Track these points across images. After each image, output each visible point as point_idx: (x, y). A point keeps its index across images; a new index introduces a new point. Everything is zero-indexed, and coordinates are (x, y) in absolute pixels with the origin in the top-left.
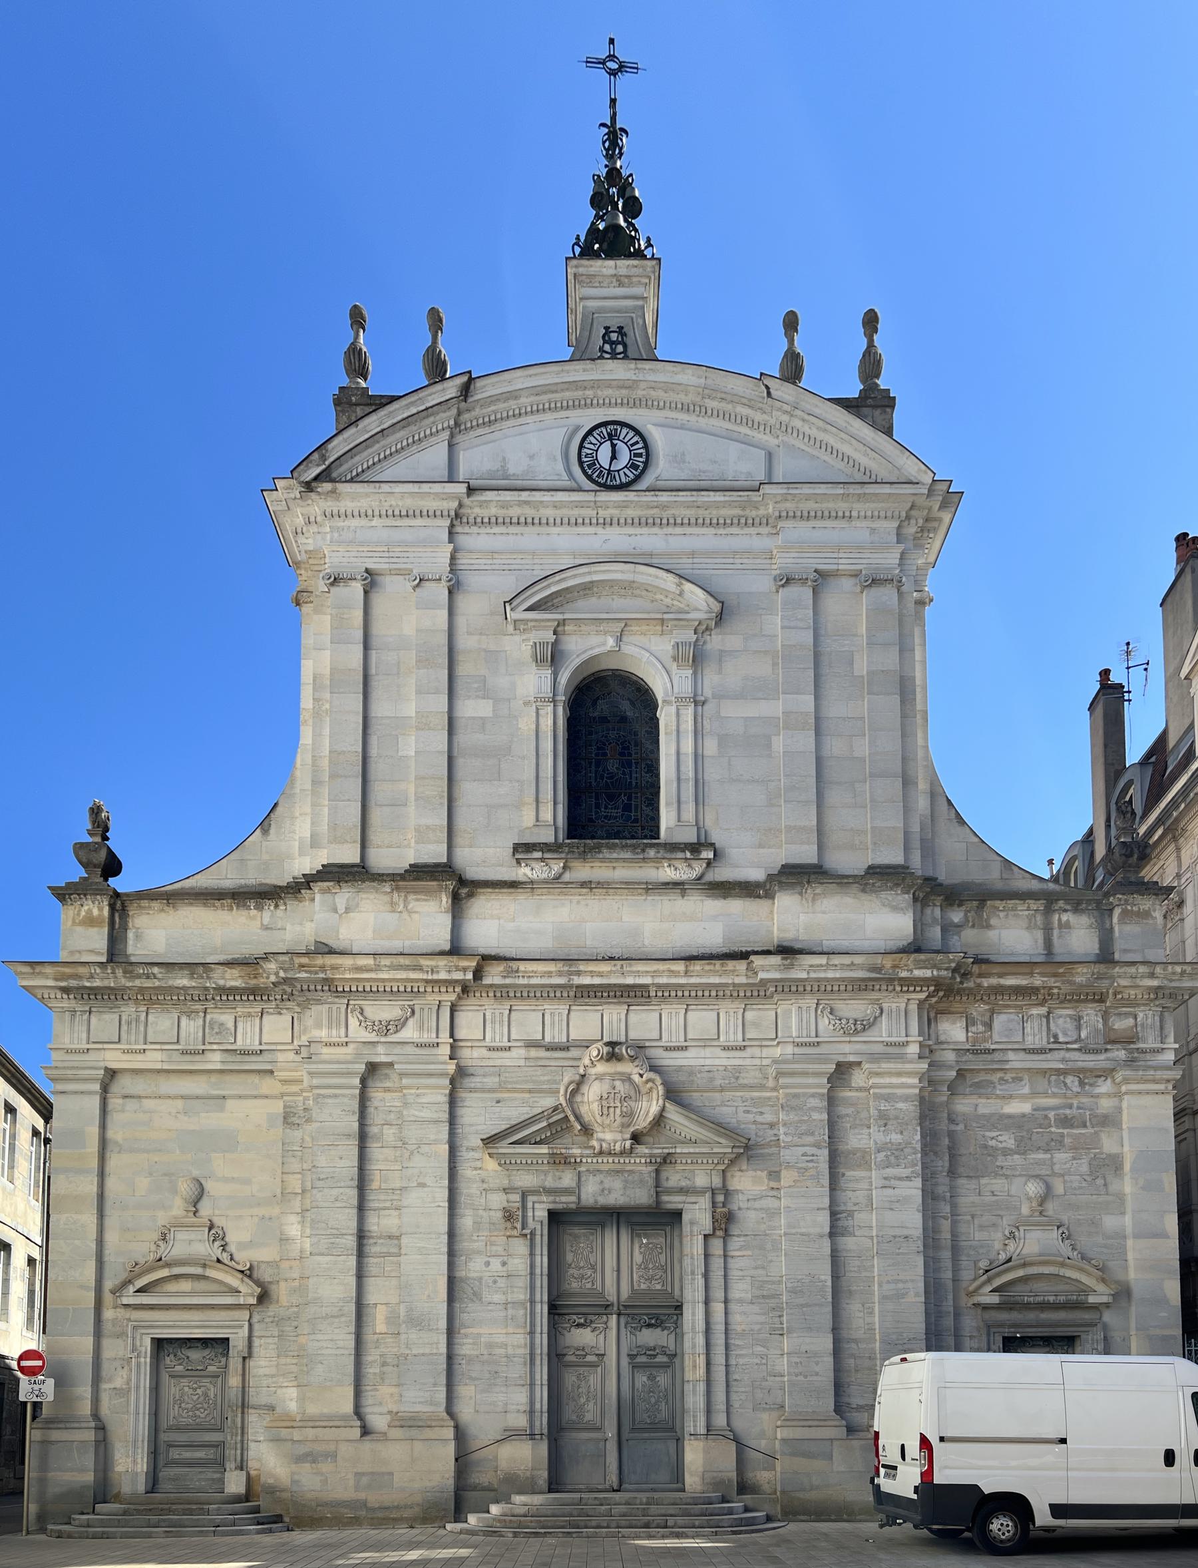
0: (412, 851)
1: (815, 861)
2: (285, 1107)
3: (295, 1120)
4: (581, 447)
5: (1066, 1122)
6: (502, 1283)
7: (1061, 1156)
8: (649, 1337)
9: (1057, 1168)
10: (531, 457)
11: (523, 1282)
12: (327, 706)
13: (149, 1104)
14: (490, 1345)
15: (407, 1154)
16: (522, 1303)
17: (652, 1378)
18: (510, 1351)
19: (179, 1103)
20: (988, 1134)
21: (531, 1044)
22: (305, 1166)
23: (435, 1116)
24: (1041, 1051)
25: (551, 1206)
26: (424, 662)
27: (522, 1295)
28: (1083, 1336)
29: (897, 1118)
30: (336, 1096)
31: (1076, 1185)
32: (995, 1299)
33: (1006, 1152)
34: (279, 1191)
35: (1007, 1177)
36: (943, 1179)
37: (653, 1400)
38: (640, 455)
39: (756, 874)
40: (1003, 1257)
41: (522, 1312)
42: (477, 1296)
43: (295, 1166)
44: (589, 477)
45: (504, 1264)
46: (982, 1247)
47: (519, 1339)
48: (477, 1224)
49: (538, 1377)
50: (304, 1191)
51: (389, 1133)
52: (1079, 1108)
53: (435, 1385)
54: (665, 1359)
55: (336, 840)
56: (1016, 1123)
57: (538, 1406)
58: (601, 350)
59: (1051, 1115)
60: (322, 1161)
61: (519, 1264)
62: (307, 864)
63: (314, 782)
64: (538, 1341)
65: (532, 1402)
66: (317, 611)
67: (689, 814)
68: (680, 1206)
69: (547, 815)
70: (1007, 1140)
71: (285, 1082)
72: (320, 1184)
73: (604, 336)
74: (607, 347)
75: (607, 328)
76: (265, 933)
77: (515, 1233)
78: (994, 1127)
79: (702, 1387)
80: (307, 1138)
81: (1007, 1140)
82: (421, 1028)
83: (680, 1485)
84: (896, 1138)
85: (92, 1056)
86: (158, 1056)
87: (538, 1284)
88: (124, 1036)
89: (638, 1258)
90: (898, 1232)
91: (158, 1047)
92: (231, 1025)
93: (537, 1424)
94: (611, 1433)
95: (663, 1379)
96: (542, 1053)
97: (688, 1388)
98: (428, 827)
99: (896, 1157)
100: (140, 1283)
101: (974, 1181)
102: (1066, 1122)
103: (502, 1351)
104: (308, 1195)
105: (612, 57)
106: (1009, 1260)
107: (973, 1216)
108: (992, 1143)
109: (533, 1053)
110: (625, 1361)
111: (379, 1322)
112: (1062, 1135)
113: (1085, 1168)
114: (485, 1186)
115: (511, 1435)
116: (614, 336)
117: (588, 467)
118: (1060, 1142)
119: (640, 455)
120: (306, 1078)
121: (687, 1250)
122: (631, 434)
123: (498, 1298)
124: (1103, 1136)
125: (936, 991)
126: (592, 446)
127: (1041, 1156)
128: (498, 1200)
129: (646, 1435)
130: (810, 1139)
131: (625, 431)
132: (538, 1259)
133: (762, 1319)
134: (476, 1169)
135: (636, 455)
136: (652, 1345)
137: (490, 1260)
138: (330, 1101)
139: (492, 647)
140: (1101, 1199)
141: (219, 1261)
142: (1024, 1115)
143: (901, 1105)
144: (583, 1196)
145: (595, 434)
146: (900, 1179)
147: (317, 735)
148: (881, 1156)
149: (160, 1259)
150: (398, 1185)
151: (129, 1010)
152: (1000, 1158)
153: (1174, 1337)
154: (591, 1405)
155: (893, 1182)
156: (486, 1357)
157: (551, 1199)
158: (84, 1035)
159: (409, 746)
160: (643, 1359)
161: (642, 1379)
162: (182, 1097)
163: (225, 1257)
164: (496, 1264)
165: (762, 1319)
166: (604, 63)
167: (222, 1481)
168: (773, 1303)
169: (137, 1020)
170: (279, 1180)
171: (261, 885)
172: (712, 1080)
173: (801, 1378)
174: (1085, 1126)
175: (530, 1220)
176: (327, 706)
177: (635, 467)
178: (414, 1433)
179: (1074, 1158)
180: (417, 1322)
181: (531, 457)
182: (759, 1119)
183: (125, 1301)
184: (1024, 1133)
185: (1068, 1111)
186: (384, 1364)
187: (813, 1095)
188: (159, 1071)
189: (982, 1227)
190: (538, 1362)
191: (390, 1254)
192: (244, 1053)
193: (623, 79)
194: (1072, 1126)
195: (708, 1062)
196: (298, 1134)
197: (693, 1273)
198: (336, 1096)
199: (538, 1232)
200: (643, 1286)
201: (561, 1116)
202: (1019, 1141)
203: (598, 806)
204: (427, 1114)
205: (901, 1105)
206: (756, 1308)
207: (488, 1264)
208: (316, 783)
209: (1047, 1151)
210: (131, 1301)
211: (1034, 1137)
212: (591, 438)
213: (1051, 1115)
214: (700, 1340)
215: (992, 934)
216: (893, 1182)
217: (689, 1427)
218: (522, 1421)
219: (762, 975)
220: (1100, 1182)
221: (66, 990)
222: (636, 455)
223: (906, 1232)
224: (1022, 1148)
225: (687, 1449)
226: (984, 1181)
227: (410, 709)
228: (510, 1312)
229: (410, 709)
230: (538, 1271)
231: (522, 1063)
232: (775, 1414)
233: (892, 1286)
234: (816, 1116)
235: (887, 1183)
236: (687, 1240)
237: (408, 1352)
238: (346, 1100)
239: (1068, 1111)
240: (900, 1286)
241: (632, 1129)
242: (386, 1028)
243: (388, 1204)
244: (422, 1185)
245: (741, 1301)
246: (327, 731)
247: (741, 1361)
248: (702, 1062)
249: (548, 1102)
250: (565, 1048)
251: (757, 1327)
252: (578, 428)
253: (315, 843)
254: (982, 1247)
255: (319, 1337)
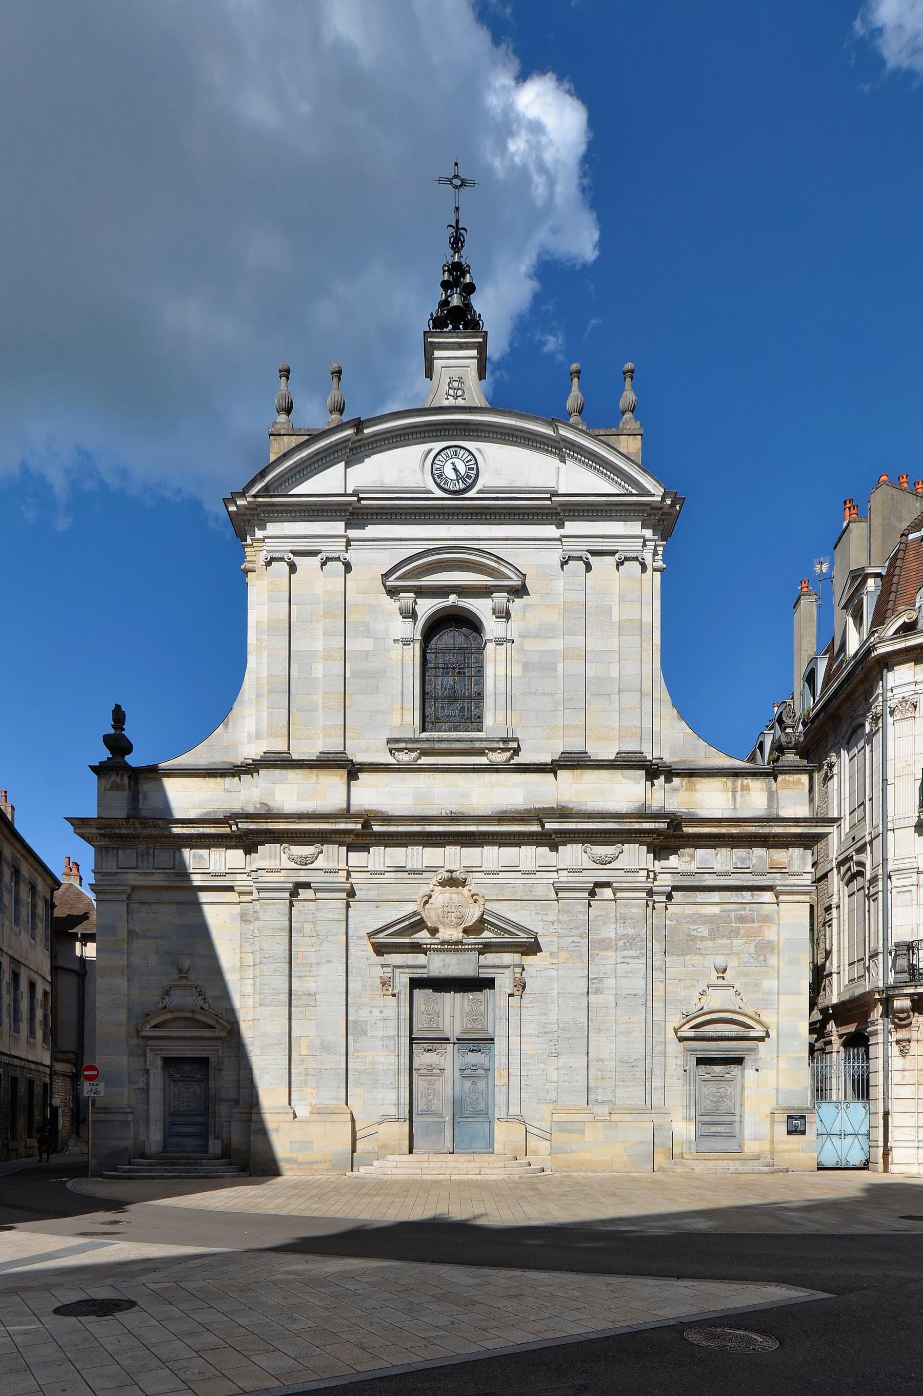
0: (321, 742)
1: (582, 749)
2: (241, 909)
3: (248, 918)
4: (433, 463)
5: (742, 919)
6: (380, 1024)
7: (737, 942)
8: (474, 1058)
9: (734, 950)
10: (400, 471)
11: (393, 1023)
12: (265, 643)
13: (155, 907)
14: (373, 1063)
15: (319, 942)
16: (392, 1038)
17: (474, 1083)
18: (385, 1067)
19: (174, 907)
20: (691, 927)
21: (400, 869)
22: (255, 949)
23: (337, 917)
24: (726, 874)
25: (412, 976)
26: (328, 614)
27: (392, 1032)
28: (747, 1057)
29: (632, 918)
30: (274, 904)
31: (746, 960)
32: (691, 1034)
33: (702, 939)
34: (239, 964)
35: (702, 955)
36: (658, 957)
37: (474, 1098)
38: (472, 469)
39: (546, 758)
40: (698, 1007)
41: (393, 1042)
42: (364, 1032)
43: (249, 948)
44: (438, 485)
45: (381, 1012)
46: (685, 1000)
47: (393, 1059)
48: (364, 987)
49: (402, 1083)
50: (254, 965)
51: (308, 927)
52: (750, 910)
53: (338, 1088)
54: (483, 1072)
55: (272, 735)
56: (709, 920)
57: (402, 1101)
58: (448, 394)
59: (732, 914)
60: (266, 946)
61: (391, 1012)
62: (252, 751)
63: (257, 696)
64: (402, 1061)
65: (399, 1098)
66: (258, 578)
67: (501, 718)
68: (493, 976)
69: (408, 718)
70: (704, 931)
71: (240, 894)
72: (265, 961)
73: (449, 384)
74: (451, 392)
75: (452, 380)
76: (229, 794)
77: (387, 993)
78: (695, 922)
79: (504, 1089)
80: (256, 931)
81: (704, 931)
82: (328, 859)
83: (491, 1150)
84: (630, 931)
85: (119, 877)
86: (162, 877)
87: (403, 1025)
88: (140, 864)
89: (467, 1008)
90: (630, 992)
91: (161, 871)
92: (206, 856)
93: (402, 1112)
94: (448, 1118)
95: (481, 1084)
96: (405, 875)
97: (497, 1089)
98: (331, 726)
99: (631, 944)
100: (153, 1023)
101: (681, 958)
102: (742, 919)
103: (381, 1067)
104: (257, 967)
105: (456, 176)
106: (702, 1009)
107: (680, 980)
108: (694, 933)
109: (400, 875)
110: (457, 1073)
111: (301, 1049)
112: (739, 928)
113: (752, 949)
114: (369, 962)
115: (385, 1119)
116: (455, 384)
117: (438, 477)
118: (737, 932)
119: (472, 469)
120: (255, 892)
121: (497, 1004)
122: (467, 454)
123: (379, 1033)
124: (765, 929)
125: (659, 835)
126: (440, 463)
127: (724, 941)
128: (378, 972)
129: (470, 1119)
130: (576, 932)
131: (462, 452)
132: (402, 1009)
133: (545, 1046)
134: (363, 951)
135: (470, 469)
136: (474, 1063)
137: (374, 1009)
138: (272, 907)
139: (374, 603)
140: (763, 969)
141: (202, 1008)
142: (715, 915)
143: (634, 910)
144: (432, 970)
145: (442, 454)
146: (633, 958)
147: (259, 663)
148: (621, 943)
149: (165, 1007)
150: (314, 961)
151: (142, 847)
152: (699, 942)
153: (804, 1058)
154: (436, 1100)
155: (628, 960)
156: (370, 1071)
157: (411, 971)
158: (115, 864)
159: (319, 670)
160: (469, 1071)
161: (468, 1084)
162: (177, 903)
163: (206, 1006)
164: (376, 1012)
165: (545, 1046)
166: (450, 180)
167: (207, 1146)
168: (551, 1036)
169: (148, 853)
170: (238, 956)
171: (223, 762)
172: (515, 893)
173: (567, 1084)
174: (753, 922)
175: (398, 984)
176: (265, 643)
177: (470, 477)
178: (326, 1117)
179: (746, 943)
180: (327, 1048)
181: (400, 471)
182: (545, 918)
183: (144, 1034)
184: (714, 927)
185: (743, 913)
186: (307, 1074)
187: (579, 904)
188: (161, 887)
189: (685, 988)
190: (402, 1074)
191: (308, 1005)
192: (216, 875)
193: (465, 190)
194: (745, 922)
195: (513, 881)
196: (251, 927)
197: (500, 1018)
198: (274, 904)
199: (403, 992)
200: (469, 1026)
201: (419, 917)
202: (711, 932)
203: (443, 708)
204: (331, 916)
205: (634, 910)
206: (540, 1040)
207: (371, 1012)
208: (259, 696)
209: (728, 938)
210: (148, 1034)
211: (721, 929)
212: (439, 457)
213: (732, 914)
214: (504, 1060)
215: (698, 796)
216: (628, 960)
217: (497, 1116)
218: (393, 1111)
219: (547, 826)
220: (762, 958)
221: (102, 835)
222: (470, 469)
223: (634, 992)
224: (713, 936)
225: (496, 1127)
226: (687, 958)
227: (319, 645)
228: (385, 1042)
229: (319, 645)
230: (402, 1017)
231: (392, 881)
232: (551, 1106)
233: (626, 1026)
234: (581, 917)
235: (624, 960)
236: (497, 997)
237: (321, 1067)
238: (280, 906)
239: (743, 913)
240: (631, 1026)
241: (463, 926)
242: (305, 861)
243: (307, 974)
244: (329, 962)
245: (531, 1035)
246: (265, 660)
247: (530, 1073)
248: (509, 881)
249: (410, 908)
250: (420, 872)
251: (540, 1052)
252: (430, 451)
253: (258, 736)
254: (685, 1000)
255: (266, 1057)
